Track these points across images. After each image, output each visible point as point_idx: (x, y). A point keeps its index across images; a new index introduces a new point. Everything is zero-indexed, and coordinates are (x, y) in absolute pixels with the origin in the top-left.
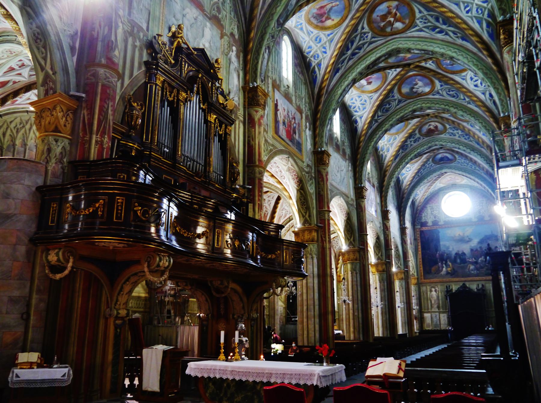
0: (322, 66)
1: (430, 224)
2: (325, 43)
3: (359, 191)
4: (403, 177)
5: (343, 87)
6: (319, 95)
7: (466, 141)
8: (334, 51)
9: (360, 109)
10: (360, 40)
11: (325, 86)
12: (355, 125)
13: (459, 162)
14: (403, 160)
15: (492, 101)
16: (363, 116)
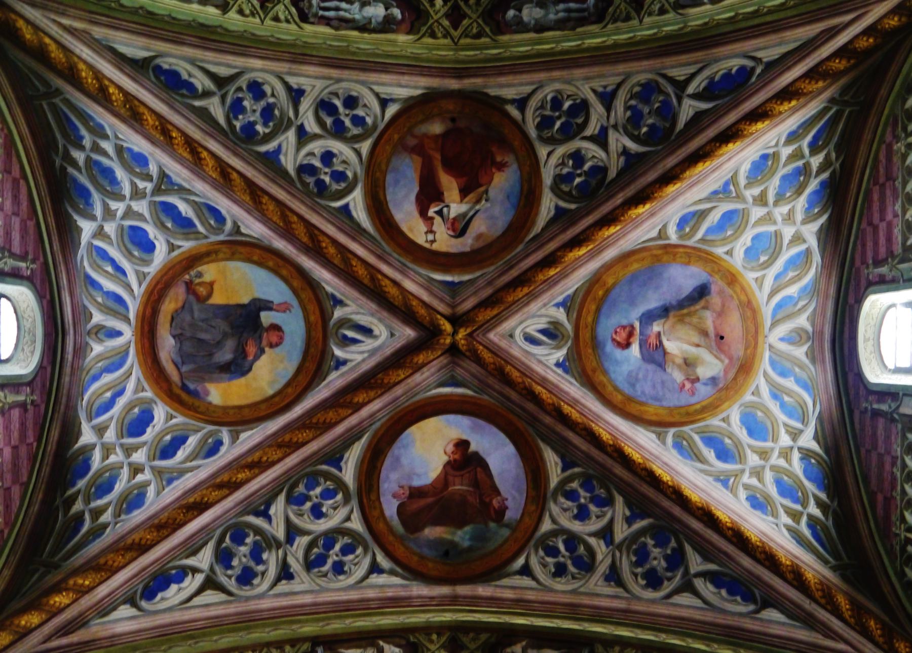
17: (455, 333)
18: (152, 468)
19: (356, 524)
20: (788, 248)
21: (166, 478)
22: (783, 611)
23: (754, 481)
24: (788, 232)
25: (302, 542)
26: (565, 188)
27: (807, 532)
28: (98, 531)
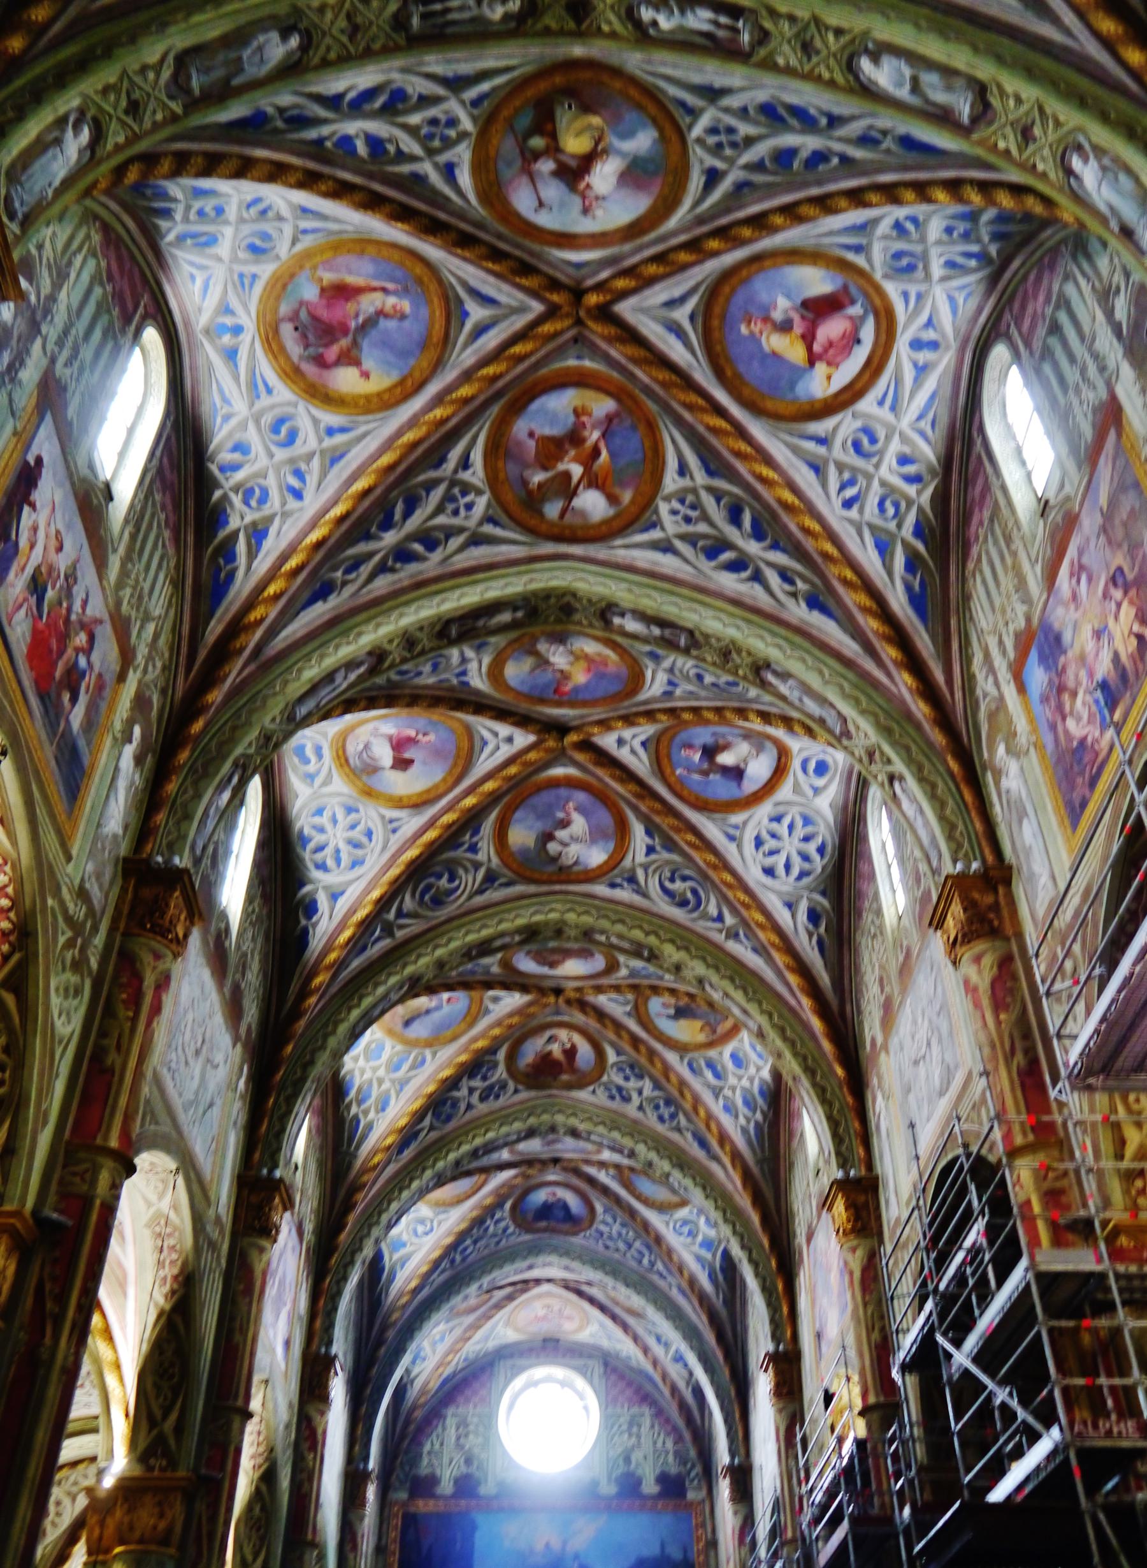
0: (268, 544)
1: (446, 1487)
2: (310, 457)
3: (254, 1199)
4: (396, 1257)
5: (329, 662)
6: (224, 650)
7: (660, 1128)
8: (335, 503)
9: (338, 861)
10: (439, 510)
11: (259, 622)
12: (303, 922)
13: (602, 1234)
14: (427, 1159)
15: (815, 939)
16: (342, 893)
24: (361, 1062)
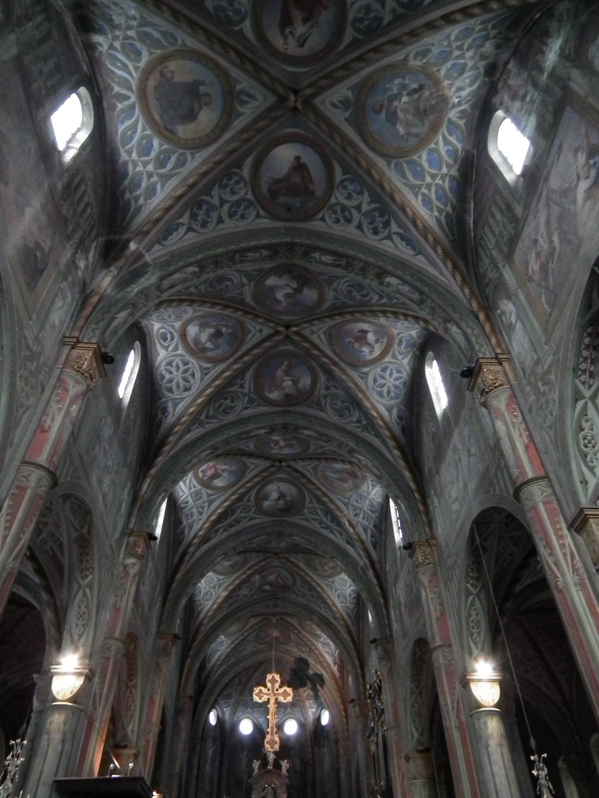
17: (296, 101)
18: (157, 174)
19: (250, 196)
20: (468, 71)
21: (165, 178)
22: (426, 258)
23: (426, 191)
25: (226, 207)
26: (359, 26)
27: (444, 221)
28: (138, 210)
